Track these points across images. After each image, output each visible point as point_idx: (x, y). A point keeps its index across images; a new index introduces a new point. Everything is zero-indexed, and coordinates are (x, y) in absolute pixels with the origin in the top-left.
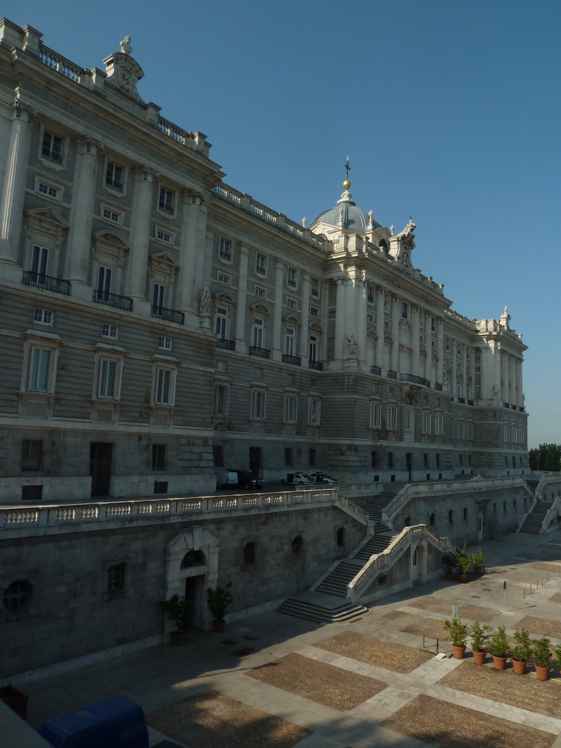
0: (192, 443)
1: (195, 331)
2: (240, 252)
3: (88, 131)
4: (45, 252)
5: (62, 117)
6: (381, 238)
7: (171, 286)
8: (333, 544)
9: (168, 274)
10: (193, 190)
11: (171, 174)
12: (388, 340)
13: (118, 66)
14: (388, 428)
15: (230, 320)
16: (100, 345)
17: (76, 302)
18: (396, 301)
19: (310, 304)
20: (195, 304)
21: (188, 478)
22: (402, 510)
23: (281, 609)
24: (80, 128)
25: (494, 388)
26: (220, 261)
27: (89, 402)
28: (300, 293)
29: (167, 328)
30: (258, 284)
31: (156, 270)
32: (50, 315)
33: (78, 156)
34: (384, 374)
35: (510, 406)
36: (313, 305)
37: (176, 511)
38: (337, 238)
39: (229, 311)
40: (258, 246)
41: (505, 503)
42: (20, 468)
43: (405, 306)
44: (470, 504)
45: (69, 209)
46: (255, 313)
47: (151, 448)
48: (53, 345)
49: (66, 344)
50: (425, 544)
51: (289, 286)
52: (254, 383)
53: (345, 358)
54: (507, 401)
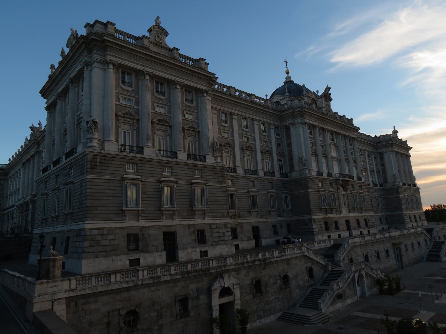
0: (218, 227)
1: (212, 165)
2: (233, 118)
3: (144, 67)
5: (129, 63)
6: (312, 98)
7: (197, 142)
8: (307, 278)
9: (194, 136)
10: (202, 89)
11: (189, 82)
12: (324, 156)
13: (155, 32)
14: (332, 207)
15: (231, 157)
16: (162, 179)
17: (148, 157)
18: (326, 132)
19: (276, 141)
20: (210, 150)
21: (218, 247)
22: (347, 254)
23: (280, 318)
24: (139, 67)
25: (395, 175)
26: (222, 125)
27: (160, 210)
28: (269, 136)
29: (197, 165)
30: (244, 134)
31: (187, 135)
32: (134, 166)
33: (140, 81)
34: (325, 175)
35: (407, 184)
36: (278, 142)
37: (213, 266)
38: (286, 102)
39: (231, 151)
40: (242, 114)
41: (412, 244)
42: (127, 250)
43: (332, 134)
44: (388, 246)
45: (138, 109)
47: (196, 232)
48: (138, 182)
49: (144, 181)
50: (363, 273)
51: (262, 133)
52: (250, 190)
53: (301, 169)
54: (405, 182)
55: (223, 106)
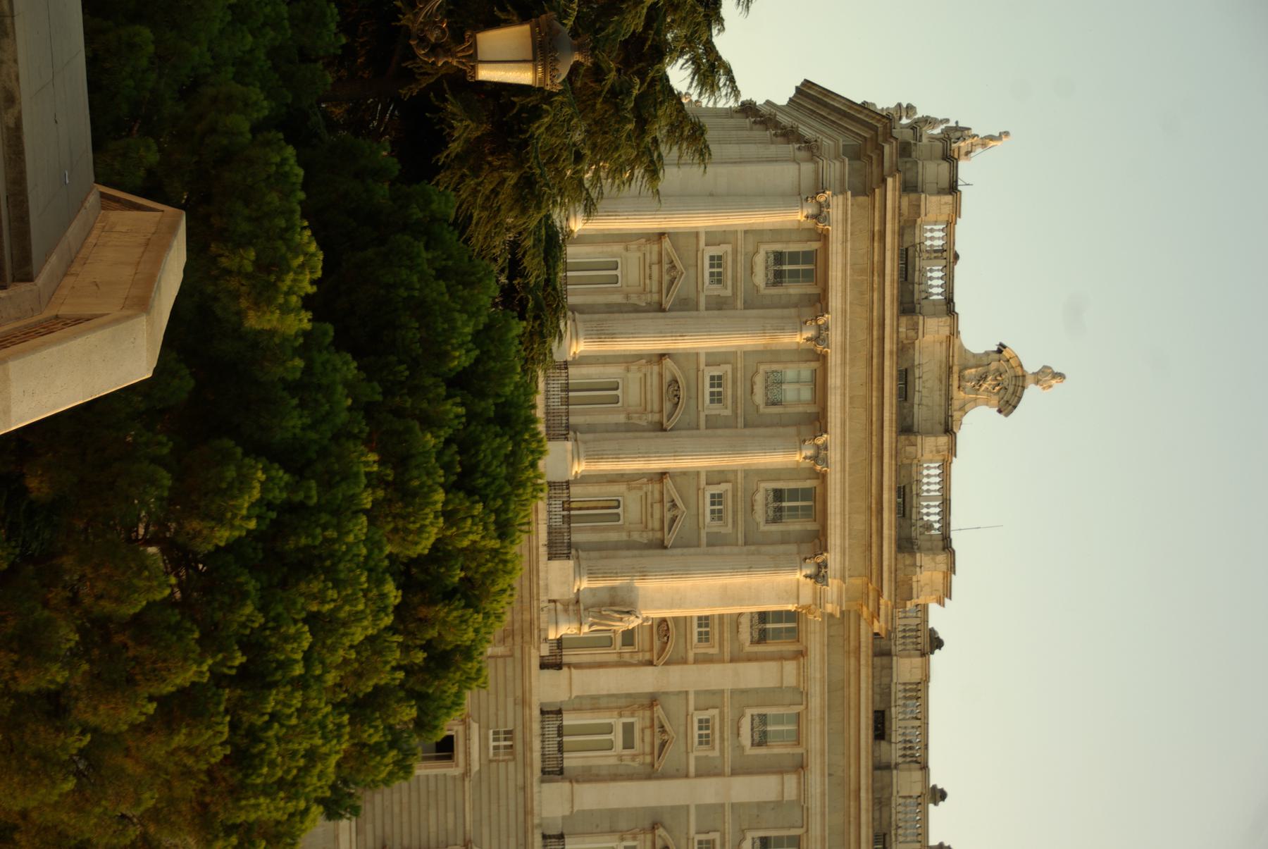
1: (541, 583)
2: (781, 771)
4: (615, 280)
7: (623, 536)
11: (838, 497)
15: (613, 761)
26: (743, 715)
39: (634, 757)
45: (697, 310)
46: (649, 844)
55: (822, 719)
